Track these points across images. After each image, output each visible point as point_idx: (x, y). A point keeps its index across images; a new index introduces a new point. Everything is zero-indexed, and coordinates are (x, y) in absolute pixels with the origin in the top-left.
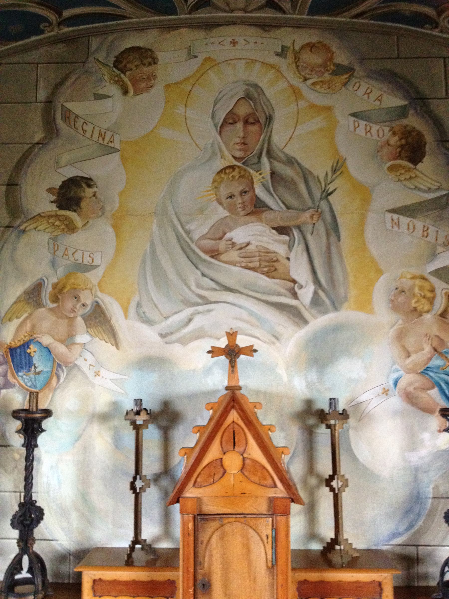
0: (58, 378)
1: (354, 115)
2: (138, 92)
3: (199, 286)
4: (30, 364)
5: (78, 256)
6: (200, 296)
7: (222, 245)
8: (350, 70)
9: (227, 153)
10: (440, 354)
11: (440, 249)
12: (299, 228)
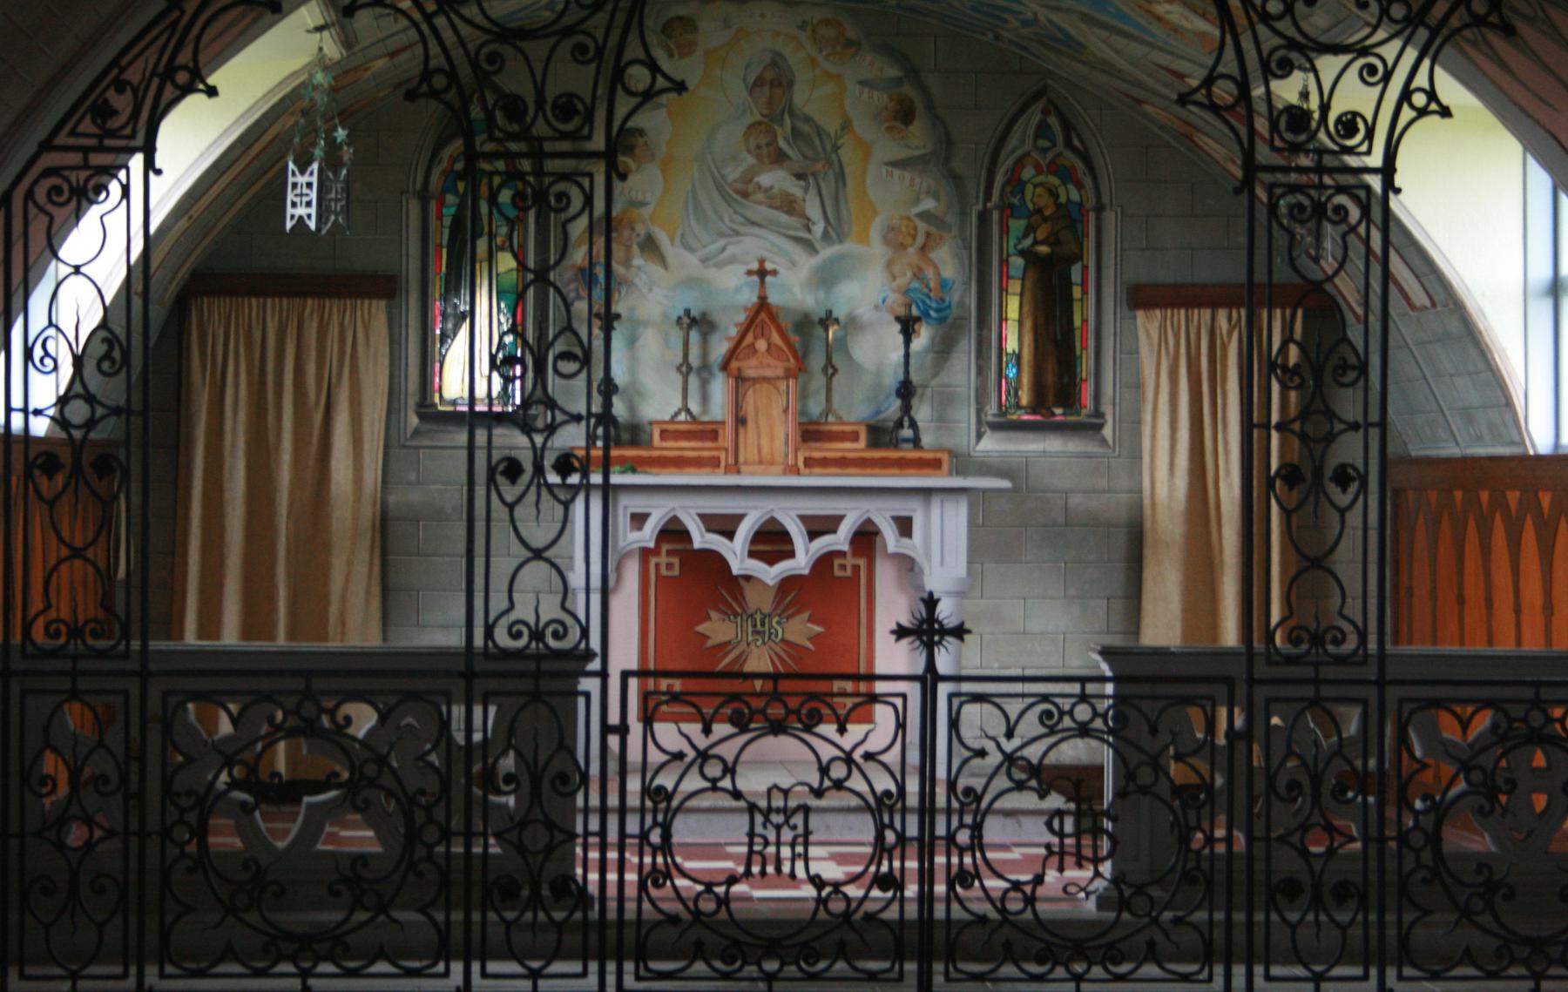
0: (620, 293)
1: (862, 83)
2: (682, 56)
3: (732, 221)
5: (633, 194)
6: (734, 230)
7: (751, 187)
9: (755, 111)
10: (918, 278)
11: (922, 196)
12: (814, 175)
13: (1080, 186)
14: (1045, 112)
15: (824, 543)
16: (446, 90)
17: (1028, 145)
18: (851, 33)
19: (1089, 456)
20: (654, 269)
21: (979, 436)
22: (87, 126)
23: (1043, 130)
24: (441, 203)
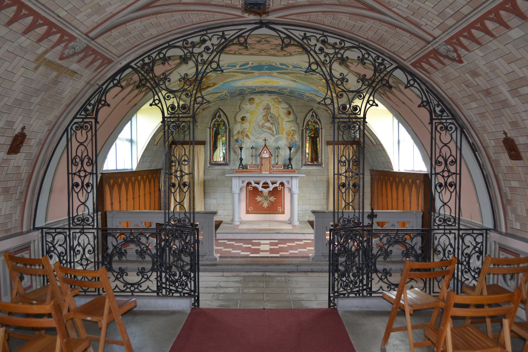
4: (238, 142)
8: (281, 102)
13: (318, 125)
14: (313, 113)
15: (275, 185)
16: (158, 104)
17: (310, 118)
18: (280, 100)
19: (320, 170)
20: (248, 139)
21: (302, 167)
22: (83, 113)
23: (312, 116)
24: (213, 129)
